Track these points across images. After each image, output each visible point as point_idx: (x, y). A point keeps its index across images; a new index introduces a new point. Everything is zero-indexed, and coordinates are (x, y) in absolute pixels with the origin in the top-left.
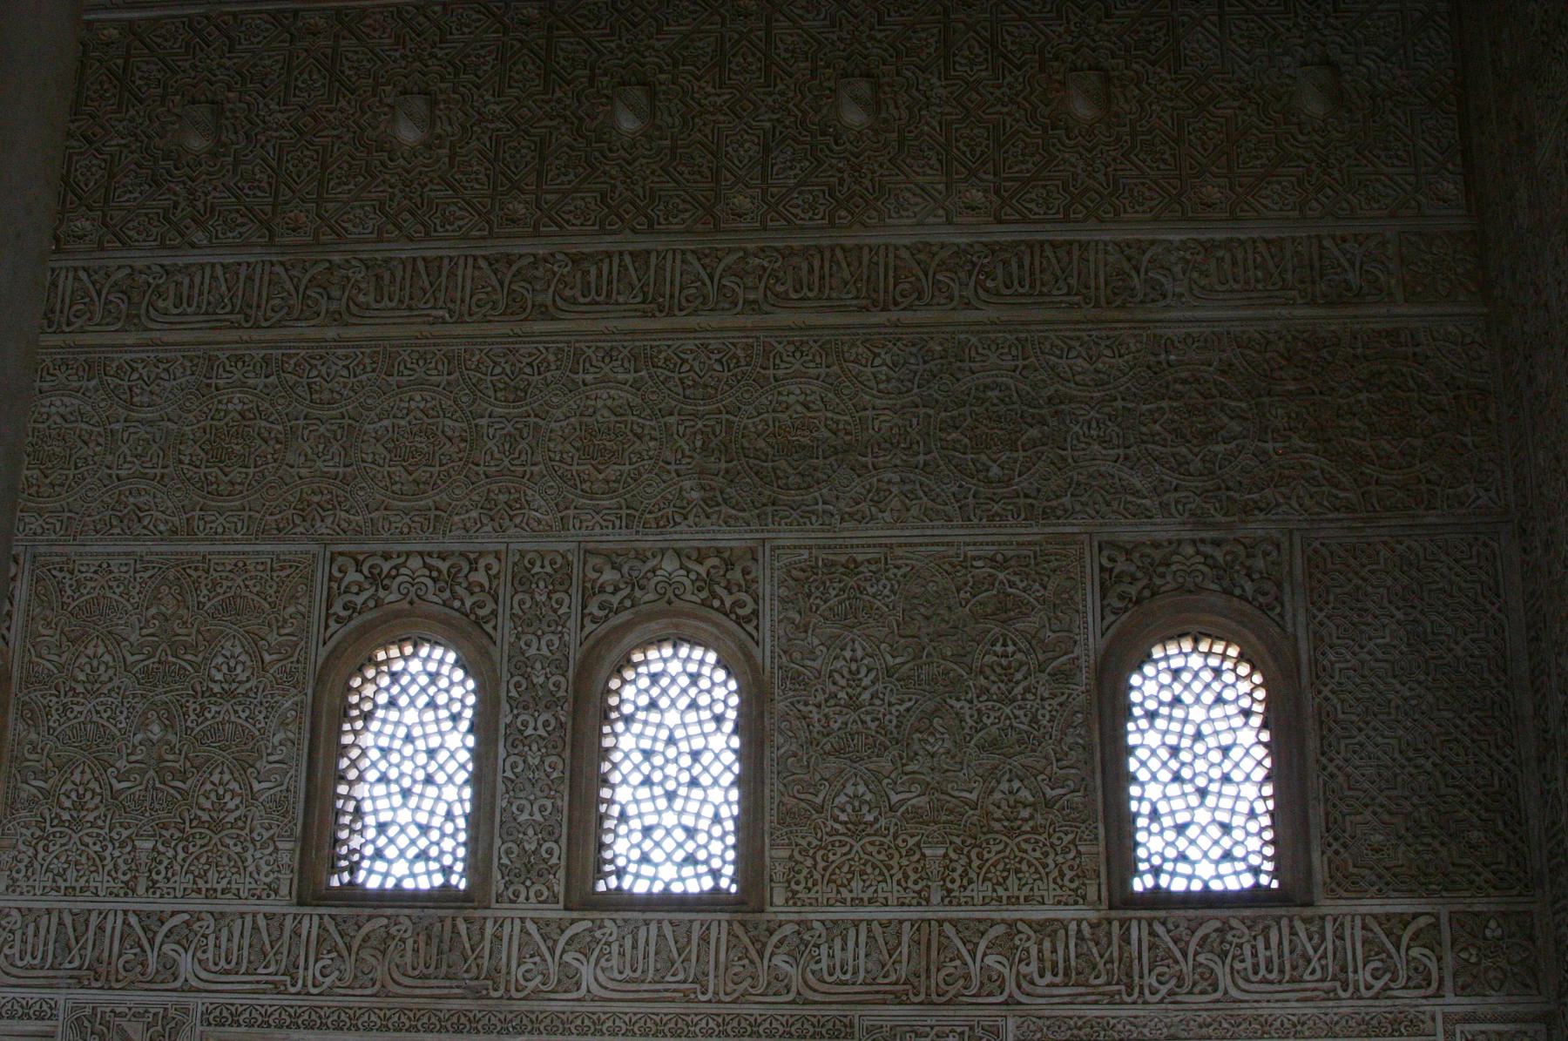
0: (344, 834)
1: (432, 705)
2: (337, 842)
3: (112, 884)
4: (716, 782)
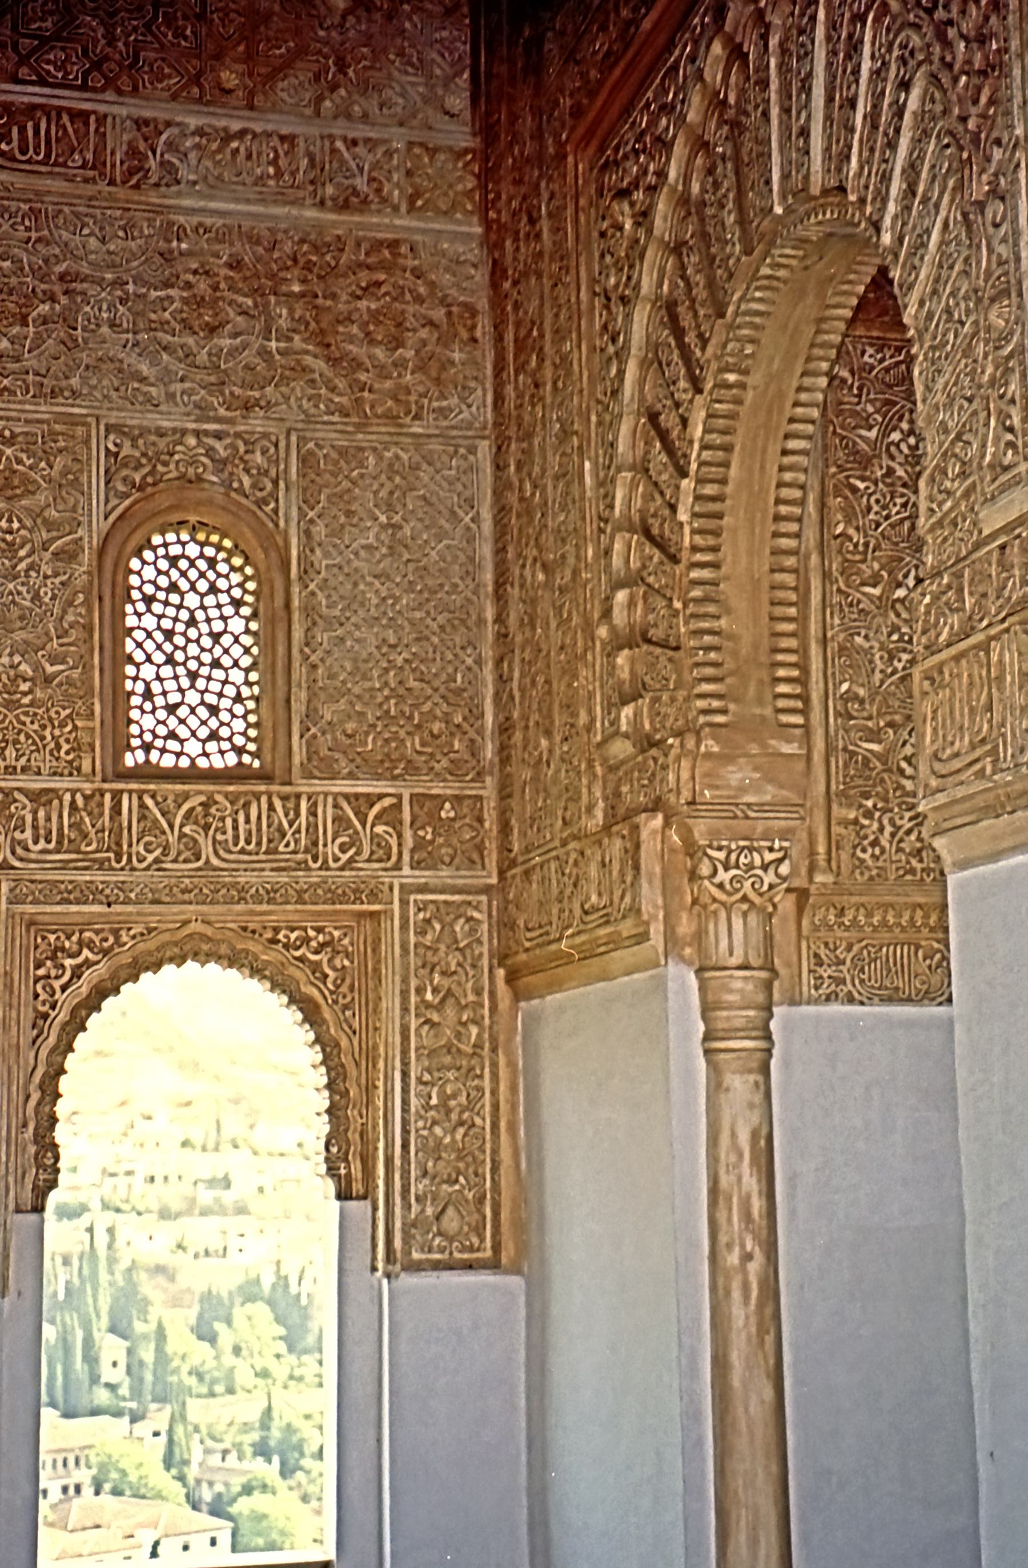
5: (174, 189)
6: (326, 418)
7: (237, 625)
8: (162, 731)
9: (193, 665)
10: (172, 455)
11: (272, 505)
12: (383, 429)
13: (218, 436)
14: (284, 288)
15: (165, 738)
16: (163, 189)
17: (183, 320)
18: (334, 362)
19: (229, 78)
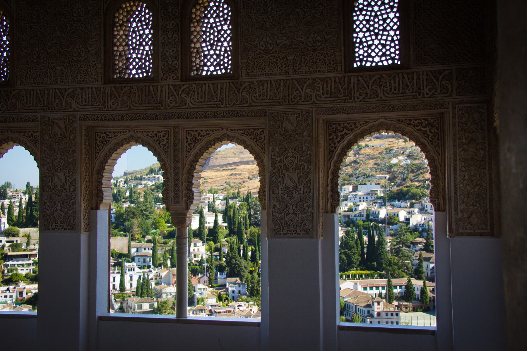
0: (357, 50)
2: (192, 62)
7: (392, 15)
8: (366, 54)
9: (376, 31)
15: (367, 57)
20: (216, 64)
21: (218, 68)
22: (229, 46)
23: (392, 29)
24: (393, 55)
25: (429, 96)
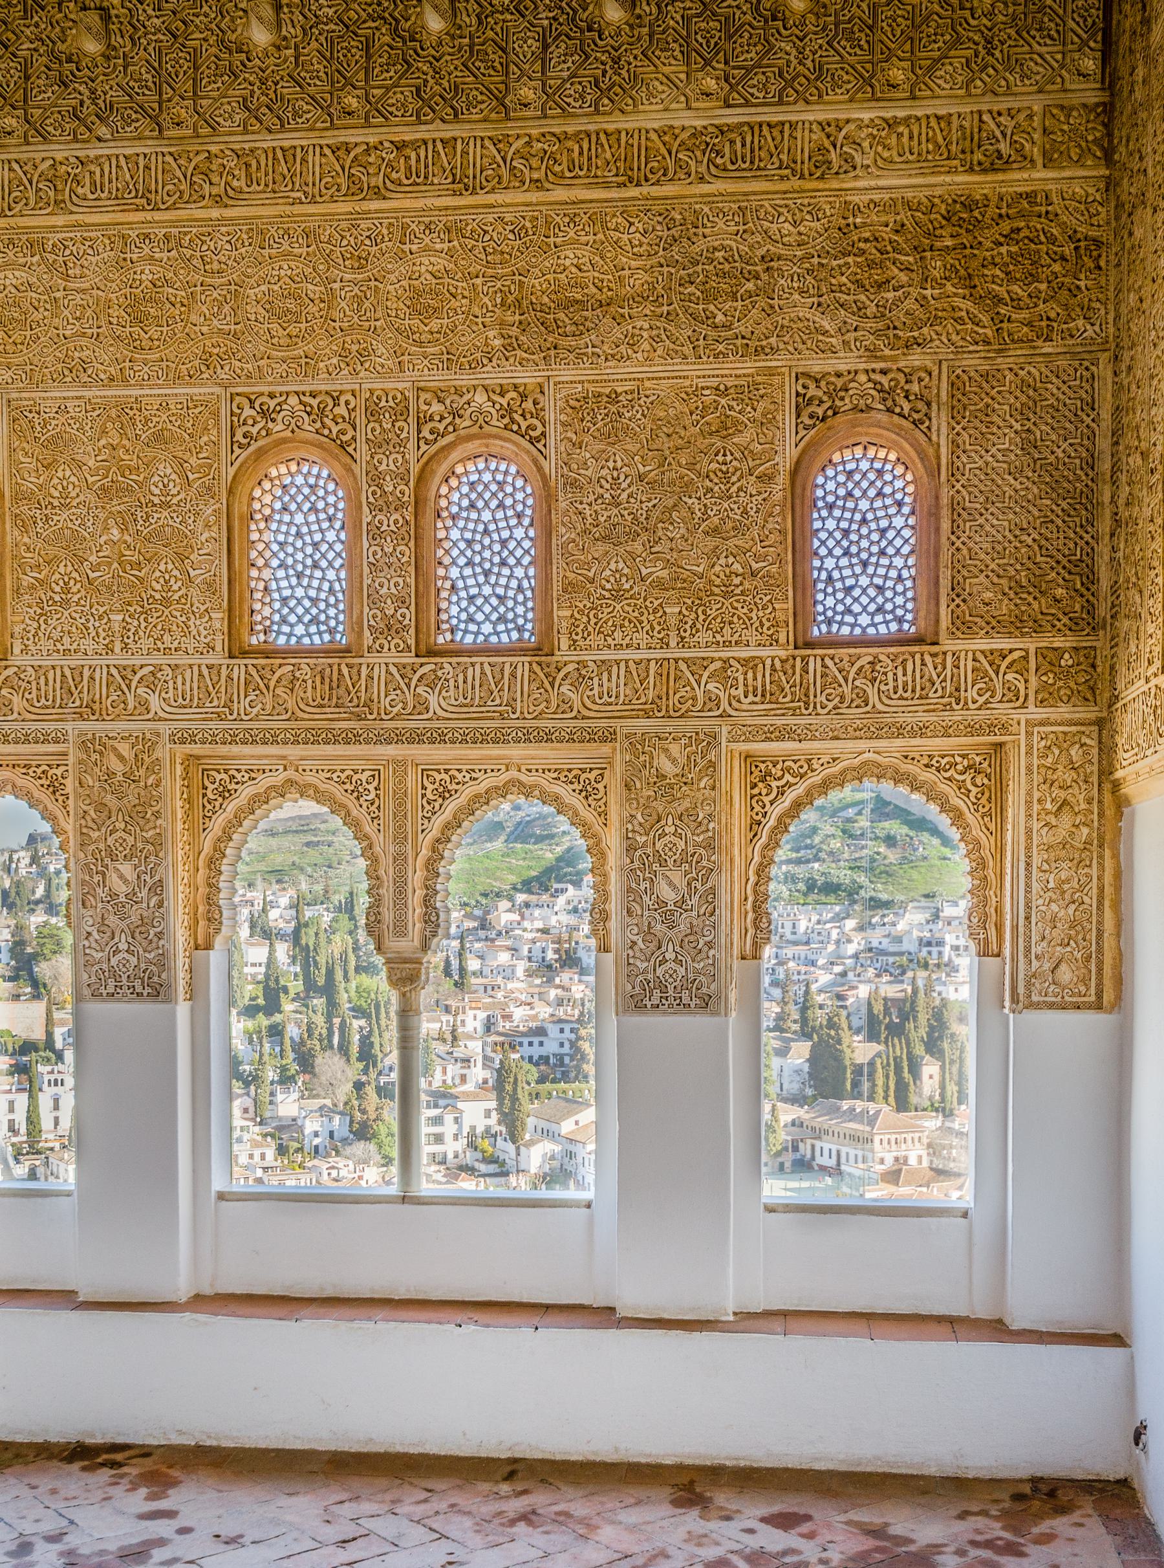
1: (314, 509)
3: (759, 637)
4: (898, 551)
5: (852, 174)
6: (971, 348)
8: (464, 616)
10: (847, 390)
11: (927, 424)
12: (1019, 352)
13: (884, 372)
14: (938, 244)
15: (466, 622)
16: (841, 176)
17: (857, 281)
18: (978, 300)
19: (898, 74)
20: (310, 621)
21: (313, 629)
22: (339, 580)
23: (519, 562)
24: (521, 621)
25: (826, 711)
